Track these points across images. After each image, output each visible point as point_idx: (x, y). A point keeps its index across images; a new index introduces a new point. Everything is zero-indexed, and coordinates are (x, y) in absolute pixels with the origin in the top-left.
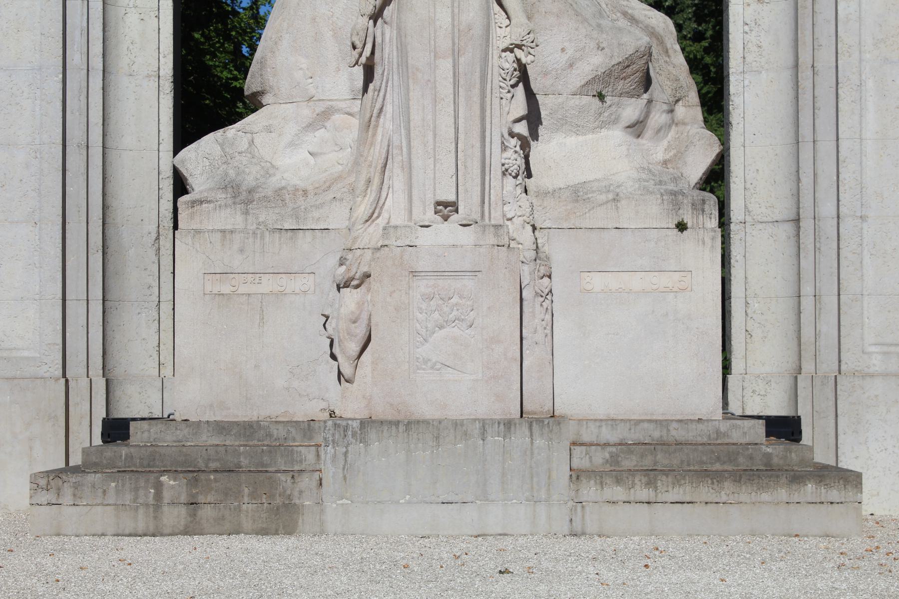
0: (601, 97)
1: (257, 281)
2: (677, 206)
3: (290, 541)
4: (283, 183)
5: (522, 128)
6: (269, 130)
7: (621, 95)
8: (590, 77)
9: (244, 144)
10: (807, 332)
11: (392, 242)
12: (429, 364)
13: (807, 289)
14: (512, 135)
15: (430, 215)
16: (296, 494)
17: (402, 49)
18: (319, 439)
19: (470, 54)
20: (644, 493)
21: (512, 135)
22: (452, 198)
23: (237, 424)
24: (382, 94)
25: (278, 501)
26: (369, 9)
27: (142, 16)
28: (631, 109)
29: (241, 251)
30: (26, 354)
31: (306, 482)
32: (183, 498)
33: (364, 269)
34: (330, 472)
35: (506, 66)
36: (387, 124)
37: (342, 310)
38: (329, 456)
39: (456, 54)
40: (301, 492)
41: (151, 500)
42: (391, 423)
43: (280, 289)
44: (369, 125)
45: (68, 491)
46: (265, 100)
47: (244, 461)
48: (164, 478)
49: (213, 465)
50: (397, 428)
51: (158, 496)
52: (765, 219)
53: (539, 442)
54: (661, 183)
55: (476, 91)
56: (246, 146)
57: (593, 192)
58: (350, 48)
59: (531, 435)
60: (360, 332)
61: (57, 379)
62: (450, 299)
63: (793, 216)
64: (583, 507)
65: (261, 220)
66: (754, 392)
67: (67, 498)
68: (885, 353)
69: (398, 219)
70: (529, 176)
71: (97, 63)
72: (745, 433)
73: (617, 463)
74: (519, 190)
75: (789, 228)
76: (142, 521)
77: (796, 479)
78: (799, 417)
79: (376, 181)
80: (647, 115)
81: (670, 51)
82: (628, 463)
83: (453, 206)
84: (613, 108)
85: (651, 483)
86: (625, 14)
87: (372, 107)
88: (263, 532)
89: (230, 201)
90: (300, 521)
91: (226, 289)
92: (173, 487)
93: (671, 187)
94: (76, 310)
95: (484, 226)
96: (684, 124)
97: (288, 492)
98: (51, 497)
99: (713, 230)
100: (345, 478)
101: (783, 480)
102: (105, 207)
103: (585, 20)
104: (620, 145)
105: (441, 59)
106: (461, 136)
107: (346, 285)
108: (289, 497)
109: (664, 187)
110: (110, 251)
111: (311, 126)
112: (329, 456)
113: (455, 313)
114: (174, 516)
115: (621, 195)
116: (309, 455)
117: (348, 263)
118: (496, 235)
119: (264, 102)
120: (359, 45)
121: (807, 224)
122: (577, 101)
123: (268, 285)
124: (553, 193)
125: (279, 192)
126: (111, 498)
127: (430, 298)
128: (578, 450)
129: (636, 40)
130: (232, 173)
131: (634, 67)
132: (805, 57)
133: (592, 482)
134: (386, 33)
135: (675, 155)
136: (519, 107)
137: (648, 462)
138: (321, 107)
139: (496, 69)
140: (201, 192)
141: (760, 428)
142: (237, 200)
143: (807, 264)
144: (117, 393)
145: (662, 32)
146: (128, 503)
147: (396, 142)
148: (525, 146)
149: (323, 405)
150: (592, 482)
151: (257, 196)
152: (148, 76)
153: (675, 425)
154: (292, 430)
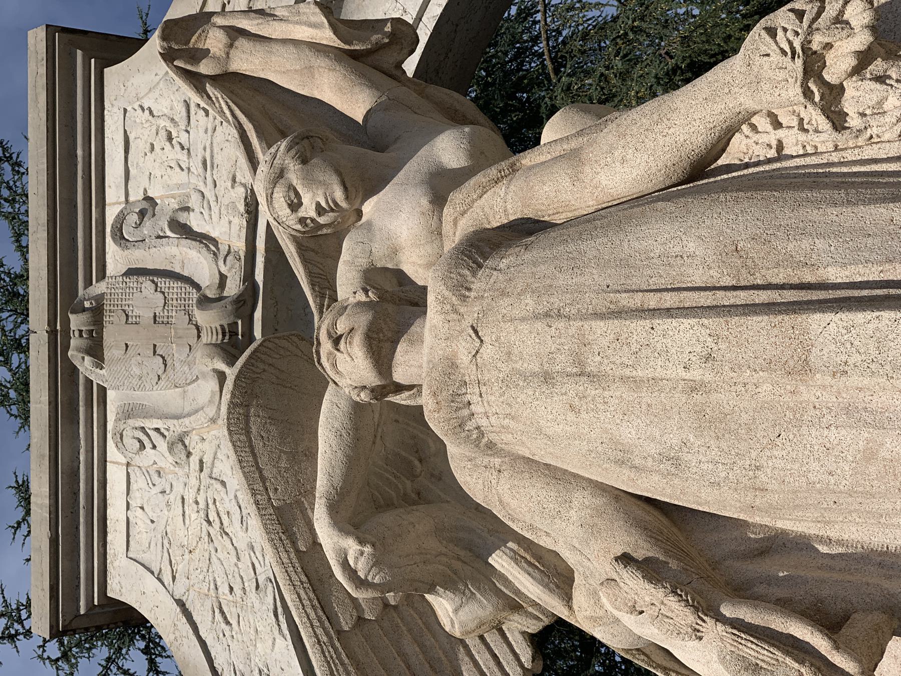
19: (820, 244)
105: (812, 358)
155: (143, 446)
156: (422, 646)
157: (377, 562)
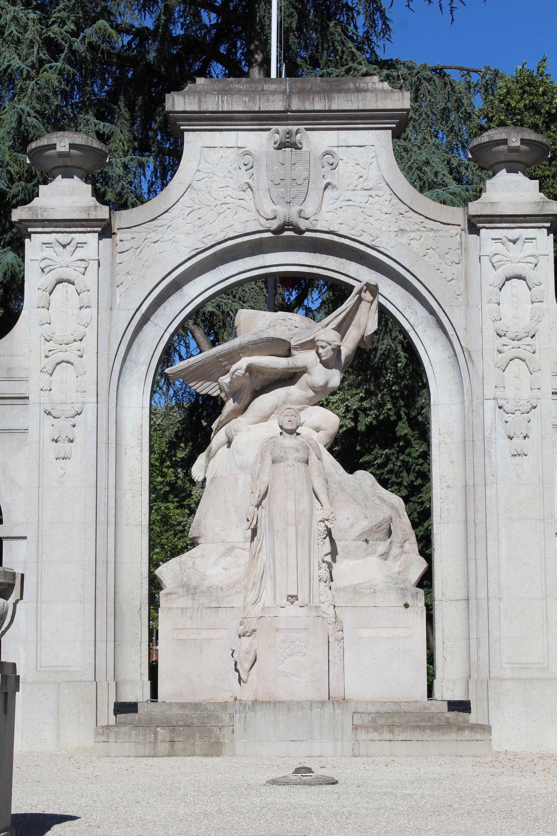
0: (367, 541)
1: (199, 633)
2: (404, 596)
3: (220, 759)
4: (211, 584)
5: (328, 559)
6: (202, 556)
7: (376, 540)
8: (361, 532)
9: (190, 564)
10: (473, 658)
11: (266, 614)
12: (285, 674)
13: (473, 635)
14: (324, 562)
15: (284, 602)
16: (221, 736)
17: (271, 521)
18: (230, 711)
20: (388, 736)
21: (324, 562)
22: (295, 594)
23: (190, 703)
24: (260, 542)
25: (213, 740)
26: (256, 503)
27: (133, 495)
28: (382, 547)
29: (191, 618)
30: (76, 669)
31: (227, 731)
32: (168, 739)
33: (253, 627)
34: (238, 726)
35: (321, 529)
36: (263, 556)
37: (242, 648)
38: (237, 718)
39: (297, 524)
40: (224, 736)
41: (152, 740)
42: (267, 702)
43: (210, 636)
44: (254, 557)
45: (112, 735)
46: (199, 541)
47: (195, 721)
48: (158, 729)
49: (180, 723)
50: (270, 705)
51: (156, 738)
52: (452, 599)
53: (338, 711)
54: (396, 583)
55: (306, 542)
56: (192, 565)
57: (364, 589)
58: (246, 520)
59: (334, 708)
60: (251, 658)
61: (92, 682)
62: (294, 642)
63: (466, 598)
64: (359, 743)
65: (200, 602)
66: (447, 688)
67: (112, 739)
68: (512, 668)
69: (269, 603)
70: (332, 580)
71: (112, 520)
72: (437, 708)
73: (375, 722)
74: (327, 588)
75: (464, 603)
76: (148, 750)
77: (460, 729)
78: (469, 701)
79: (258, 584)
80: (390, 549)
81: (402, 516)
82: (381, 722)
83: (295, 597)
84: (373, 547)
85: (391, 731)
86: (379, 497)
87: (256, 548)
88: (206, 755)
89: (185, 593)
90: (223, 750)
91: (183, 637)
92: (162, 733)
93: (402, 586)
94: (101, 646)
95: (311, 607)
96: (409, 553)
97: (218, 736)
98: (104, 738)
99: (422, 607)
100: (245, 729)
101: (454, 729)
102: (115, 593)
103: (359, 504)
104: (376, 565)
106: (299, 563)
107: (244, 636)
108: (218, 738)
109: (398, 586)
110: (117, 616)
111: (224, 555)
112: (237, 718)
113: (297, 649)
114: (163, 747)
115: (377, 590)
116: (227, 719)
117: (244, 624)
118: (317, 611)
119: (199, 542)
120: (250, 519)
121: (472, 602)
122: (355, 543)
123: (204, 635)
124: (344, 589)
125: (209, 588)
126: (133, 739)
127: (284, 642)
128: (356, 716)
129: (383, 513)
130: (185, 579)
131: (383, 527)
132: (471, 517)
133: (363, 731)
134: (263, 513)
135: (404, 569)
136: (327, 548)
137: (390, 722)
138: (228, 546)
139: (316, 530)
140: (171, 589)
141: (445, 706)
142: (189, 593)
143: (473, 622)
144: (120, 689)
145: (397, 506)
146: (141, 741)
147: (268, 566)
148: (330, 566)
149: (231, 694)
150: (363, 731)
151: (199, 590)
152: (136, 525)
153: (404, 704)
154: (217, 706)
155: (245, 165)
156: (215, 372)
157: (238, 377)
